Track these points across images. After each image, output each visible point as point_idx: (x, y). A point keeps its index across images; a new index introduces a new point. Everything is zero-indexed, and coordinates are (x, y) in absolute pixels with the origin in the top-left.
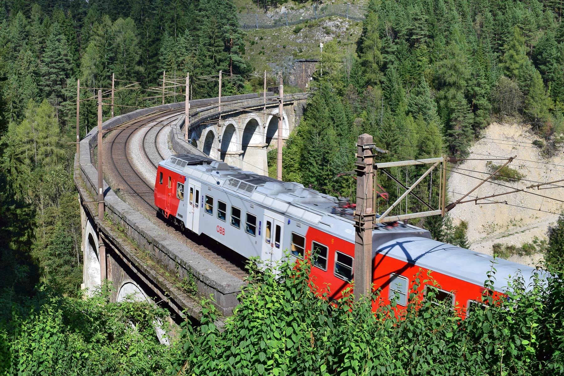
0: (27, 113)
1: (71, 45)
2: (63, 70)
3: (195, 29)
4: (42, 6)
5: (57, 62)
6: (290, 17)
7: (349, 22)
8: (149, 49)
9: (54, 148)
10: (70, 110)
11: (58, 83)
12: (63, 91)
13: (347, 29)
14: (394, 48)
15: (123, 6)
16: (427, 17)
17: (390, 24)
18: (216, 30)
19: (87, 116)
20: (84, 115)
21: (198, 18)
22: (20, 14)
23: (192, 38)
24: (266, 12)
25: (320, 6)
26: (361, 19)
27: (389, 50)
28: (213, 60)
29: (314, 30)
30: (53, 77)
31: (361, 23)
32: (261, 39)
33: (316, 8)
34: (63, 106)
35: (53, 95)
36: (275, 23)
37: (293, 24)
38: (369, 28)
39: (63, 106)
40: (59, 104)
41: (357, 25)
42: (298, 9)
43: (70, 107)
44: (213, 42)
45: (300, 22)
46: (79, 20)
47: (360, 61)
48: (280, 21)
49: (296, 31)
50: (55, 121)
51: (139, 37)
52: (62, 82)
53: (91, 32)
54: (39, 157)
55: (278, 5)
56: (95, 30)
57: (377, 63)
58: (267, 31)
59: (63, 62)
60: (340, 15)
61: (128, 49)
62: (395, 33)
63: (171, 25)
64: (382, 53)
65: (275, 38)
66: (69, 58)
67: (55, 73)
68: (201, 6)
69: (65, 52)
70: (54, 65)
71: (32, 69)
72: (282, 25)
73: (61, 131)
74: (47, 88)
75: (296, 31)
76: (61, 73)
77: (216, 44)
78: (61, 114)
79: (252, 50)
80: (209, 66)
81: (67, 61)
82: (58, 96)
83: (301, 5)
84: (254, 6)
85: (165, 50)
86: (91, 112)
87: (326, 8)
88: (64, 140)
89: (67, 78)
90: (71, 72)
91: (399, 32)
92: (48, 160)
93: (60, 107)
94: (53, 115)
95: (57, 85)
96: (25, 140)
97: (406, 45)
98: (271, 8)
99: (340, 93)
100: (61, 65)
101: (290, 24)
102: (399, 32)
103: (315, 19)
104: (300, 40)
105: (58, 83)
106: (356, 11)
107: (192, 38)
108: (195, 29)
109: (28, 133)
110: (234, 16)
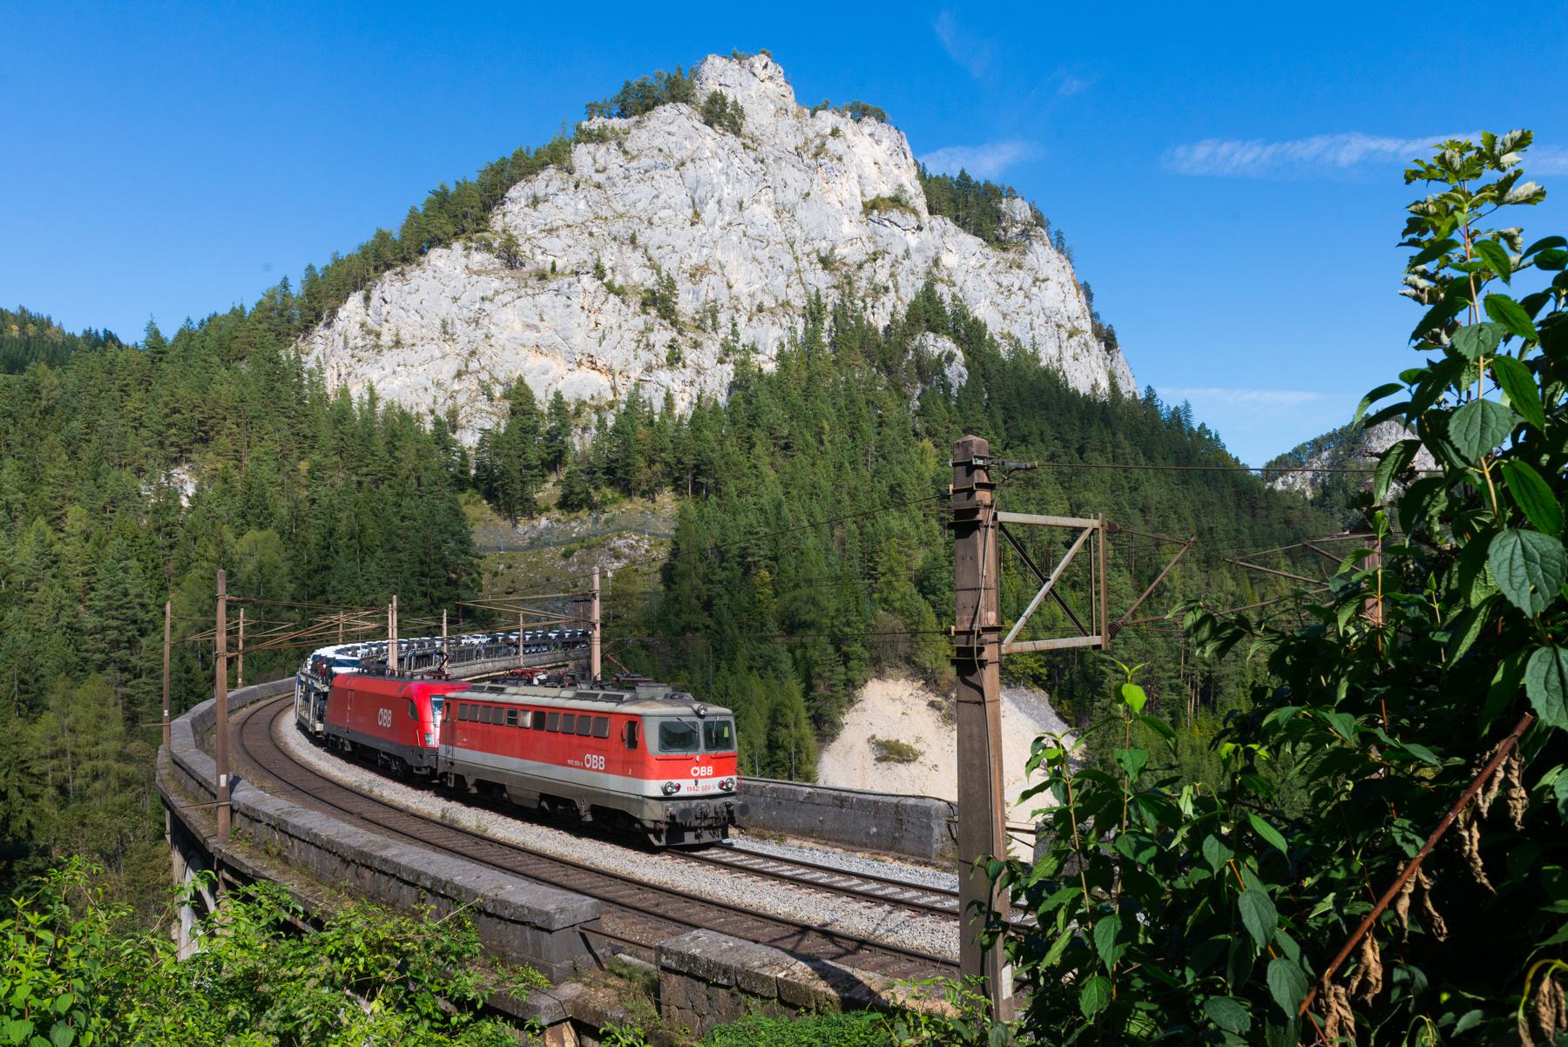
0: (52, 701)
1: (151, 578)
2: (135, 622)
3: (393, 549)
4: (91, 510)
5: (121, 607)
6: (556, 533)
7: (649, 540)
8: (309, 582)
9: (111, 762)
10: (148, 693)
11: (122, 645)
12: (134, 659)
13: (647, 551)
14: (723, 575)
15: (257, 511)
16: (767, 530)
17: (712, 541)
18: (433, 551)
19: (186, 699)
20: (179, 699)
21: (400, 532)
22: (41, 522)
23: (389, 564)
24: (515, 526)
25: (604, 517)
26: (667, 536)
27: (715, 578)
28: (428, 600)
29: (596, 553)
30: (112, 634)
31: (668, 542)
32: (510, 567)
33: (596, 520)
34: (132, 687)
35: (110, 669)
36: (532, 543)
37: (561, 544)
38: (683, 546)
39: (132, 687)
40: (124, 684)
41: (661, 544)
42: (569, 522)
43: (147, 688)
44: (426, 569)
45: (572, 540)
46: (169, 535)
47: (672, 595)
48: (539, 539)
49: (567, 555)
50: (116, 713)
51: (291, 563)
52: (132, 644)
53: (193, 555)
54: (78, 782)
55: (536, 515)
56: (201, 551)
57: (698, 598)
58: (518, 554)
59: (133, 608)
60: (635, 530)
61: (269, 582)
62: (722, 555)
63: (350, 543)
64: (704, 583)
65: (532, 566)
66: (146, 600)
67: (117, 628)
68: (405, 512)
69: (139, 590)
70: (114, 613)
71: (64, 620)
72: (542, 547)
73: (129, 732)
74: (97, 656)
75: (567, 555)
76: (130, 627)
77: (432, 574)
78: (130, 701)
79: (494, 585)
80: (420, 608)
81: (143, 605)
82: (123, 670)
83: (573, 515)
84: (495, 516)
85: (340, 582)
86: (193, 692)
87: (612, 520)
88: (135, 746)
89: (142, 635)
90: (151, 627)
91: (727, 551)
92: (98, 785)
93: (128, 690)
94: (111, 701)
95: (119, 648)
96: (48, 750)
97: (739, 571)
98: (523, 520)
99: (644, 646)
100: (130, 613)
101: (555, 544)
102: (727, 551)
103: (596, 535)
104: (574, 569)
105: (122, 645)
106: (659, 524)
107: (389, 564)
108: (393, 549)
109: (54, 738)
110: (464, 527)
